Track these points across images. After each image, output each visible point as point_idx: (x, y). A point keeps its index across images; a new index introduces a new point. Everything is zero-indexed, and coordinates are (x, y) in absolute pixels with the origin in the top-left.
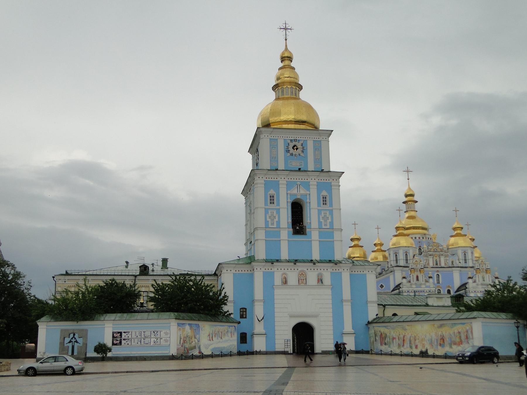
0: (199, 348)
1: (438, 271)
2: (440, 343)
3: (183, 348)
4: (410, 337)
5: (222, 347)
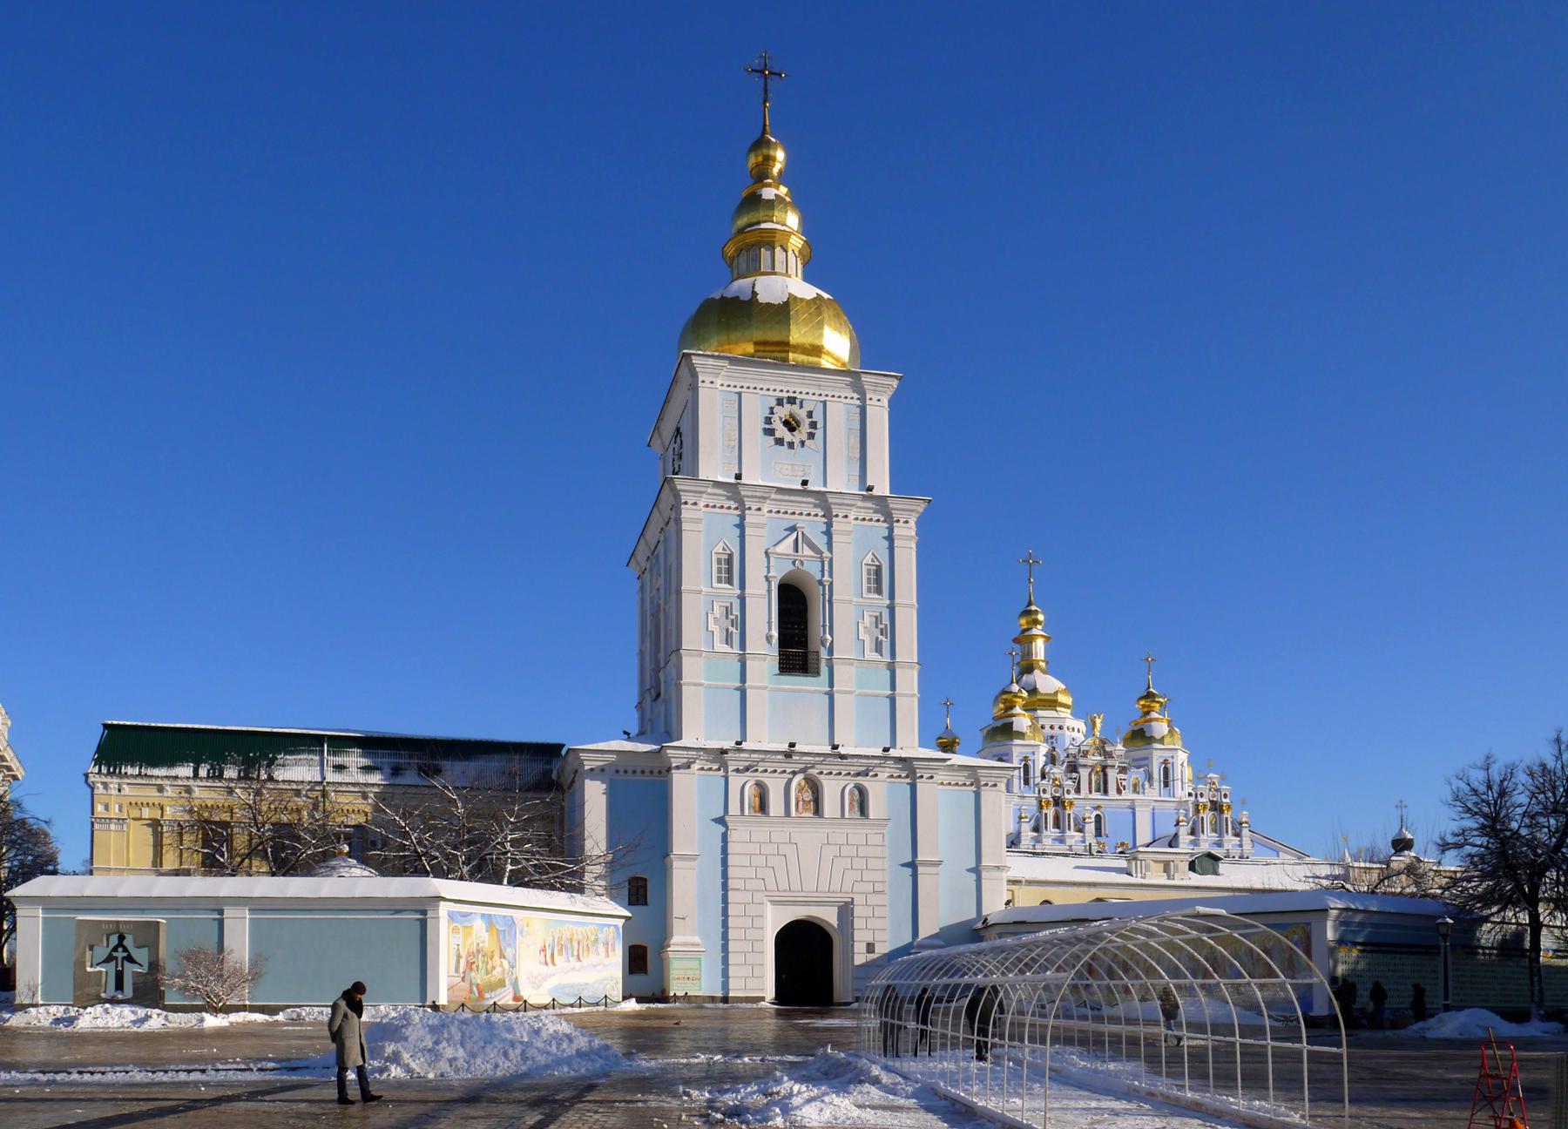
0: (515, 985)
1: (1098, 808)
3: (466, 985)
5: (580, 985)
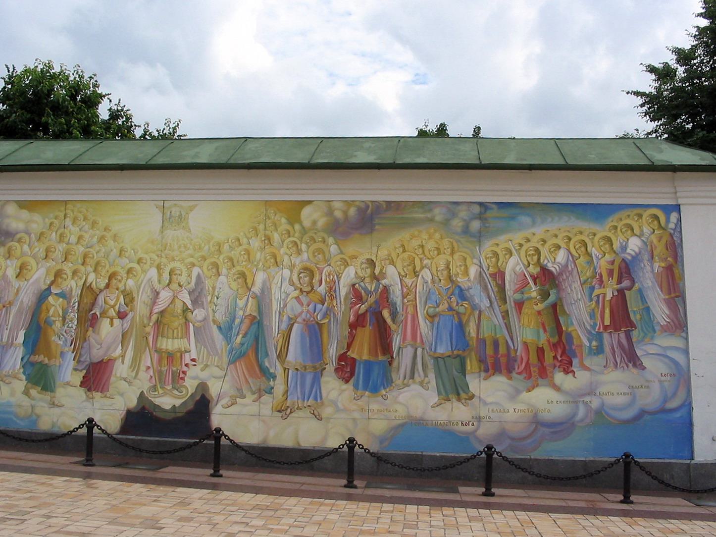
2: (342, 357)
4: (42, 297)
